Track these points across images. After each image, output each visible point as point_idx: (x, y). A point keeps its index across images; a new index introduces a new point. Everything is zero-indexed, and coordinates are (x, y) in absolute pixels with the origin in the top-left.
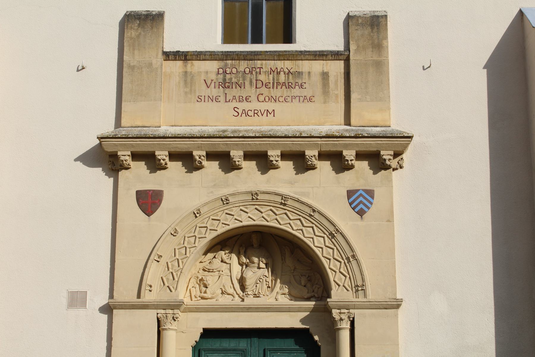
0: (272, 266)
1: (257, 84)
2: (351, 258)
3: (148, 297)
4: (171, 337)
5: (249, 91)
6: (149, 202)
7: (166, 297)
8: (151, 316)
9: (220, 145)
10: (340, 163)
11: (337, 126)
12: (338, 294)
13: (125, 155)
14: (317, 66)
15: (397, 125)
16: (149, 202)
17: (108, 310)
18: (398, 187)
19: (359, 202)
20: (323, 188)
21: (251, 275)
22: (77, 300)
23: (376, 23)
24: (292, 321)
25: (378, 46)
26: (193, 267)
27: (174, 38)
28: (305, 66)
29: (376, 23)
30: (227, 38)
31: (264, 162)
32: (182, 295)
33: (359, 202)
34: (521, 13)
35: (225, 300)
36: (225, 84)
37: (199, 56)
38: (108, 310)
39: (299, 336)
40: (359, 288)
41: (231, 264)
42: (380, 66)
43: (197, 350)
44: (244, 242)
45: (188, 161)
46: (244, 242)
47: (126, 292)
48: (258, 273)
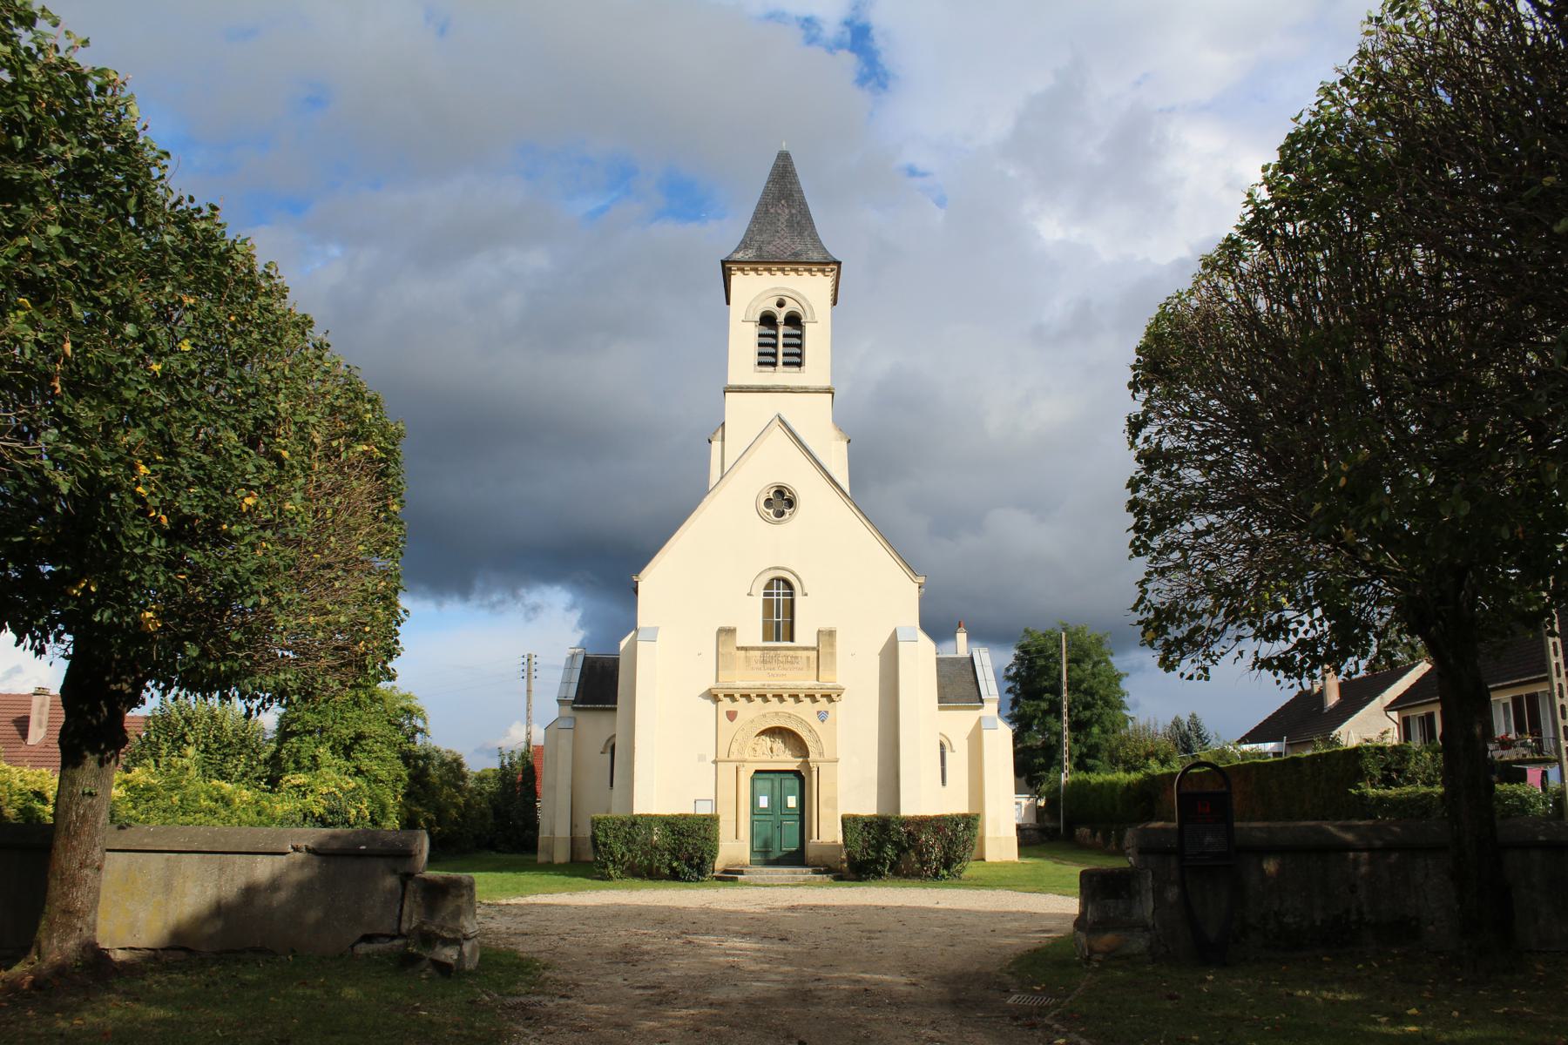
0: (784, 743)
1: (778, 662)
2: (818, 741)
3: (732, 757)
4: (742, 774)
5: (774, 665)
6: (732, 716)
7: (740, 757)
8: (734, 765)
9: (762, 692)
10: (813, 698)
11: (812, 683)
12: (812, 756)
13: (721, 696)
14: (805, 654)
15: (839, 683)
16: (732, 716)
17: (715, 762)
18: (839, 709)
19: (822, 716)
20: (806, 710)
21: (775, 747)
22: (702, 758)
23: (831, 634)
24: (794, 767)
25: (832, 645)
26: (751, 743)
27: (741, 640)
28: (799, 653)
29: (831, 634)
30: (765, 639)
31: (780, 697)
32: (746, 757)
33: (822, 716)
34: (894, 636)
35: (764, 758)
36: (764, 662)
37: (753, 648)
38: (715, 762)
39: (797, 773)
40: (821, 754)
41: (767, 741)
42: (833, 654)
43: (753, 779)
44: (773, 732)
45: (748, 697)
46: (773, 732)
47: (723, 755)
48: (778, 745)
